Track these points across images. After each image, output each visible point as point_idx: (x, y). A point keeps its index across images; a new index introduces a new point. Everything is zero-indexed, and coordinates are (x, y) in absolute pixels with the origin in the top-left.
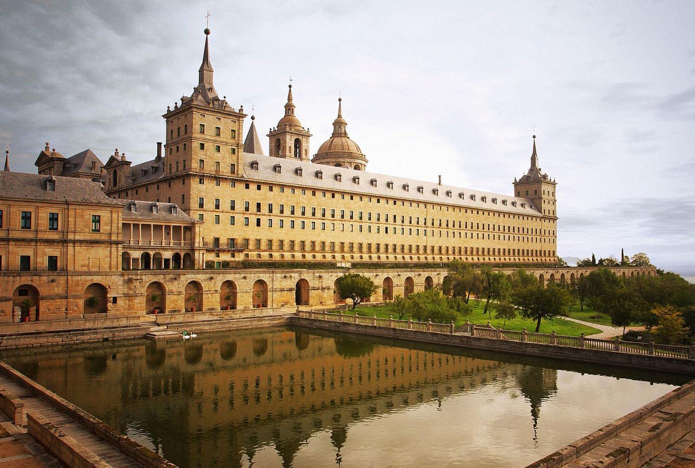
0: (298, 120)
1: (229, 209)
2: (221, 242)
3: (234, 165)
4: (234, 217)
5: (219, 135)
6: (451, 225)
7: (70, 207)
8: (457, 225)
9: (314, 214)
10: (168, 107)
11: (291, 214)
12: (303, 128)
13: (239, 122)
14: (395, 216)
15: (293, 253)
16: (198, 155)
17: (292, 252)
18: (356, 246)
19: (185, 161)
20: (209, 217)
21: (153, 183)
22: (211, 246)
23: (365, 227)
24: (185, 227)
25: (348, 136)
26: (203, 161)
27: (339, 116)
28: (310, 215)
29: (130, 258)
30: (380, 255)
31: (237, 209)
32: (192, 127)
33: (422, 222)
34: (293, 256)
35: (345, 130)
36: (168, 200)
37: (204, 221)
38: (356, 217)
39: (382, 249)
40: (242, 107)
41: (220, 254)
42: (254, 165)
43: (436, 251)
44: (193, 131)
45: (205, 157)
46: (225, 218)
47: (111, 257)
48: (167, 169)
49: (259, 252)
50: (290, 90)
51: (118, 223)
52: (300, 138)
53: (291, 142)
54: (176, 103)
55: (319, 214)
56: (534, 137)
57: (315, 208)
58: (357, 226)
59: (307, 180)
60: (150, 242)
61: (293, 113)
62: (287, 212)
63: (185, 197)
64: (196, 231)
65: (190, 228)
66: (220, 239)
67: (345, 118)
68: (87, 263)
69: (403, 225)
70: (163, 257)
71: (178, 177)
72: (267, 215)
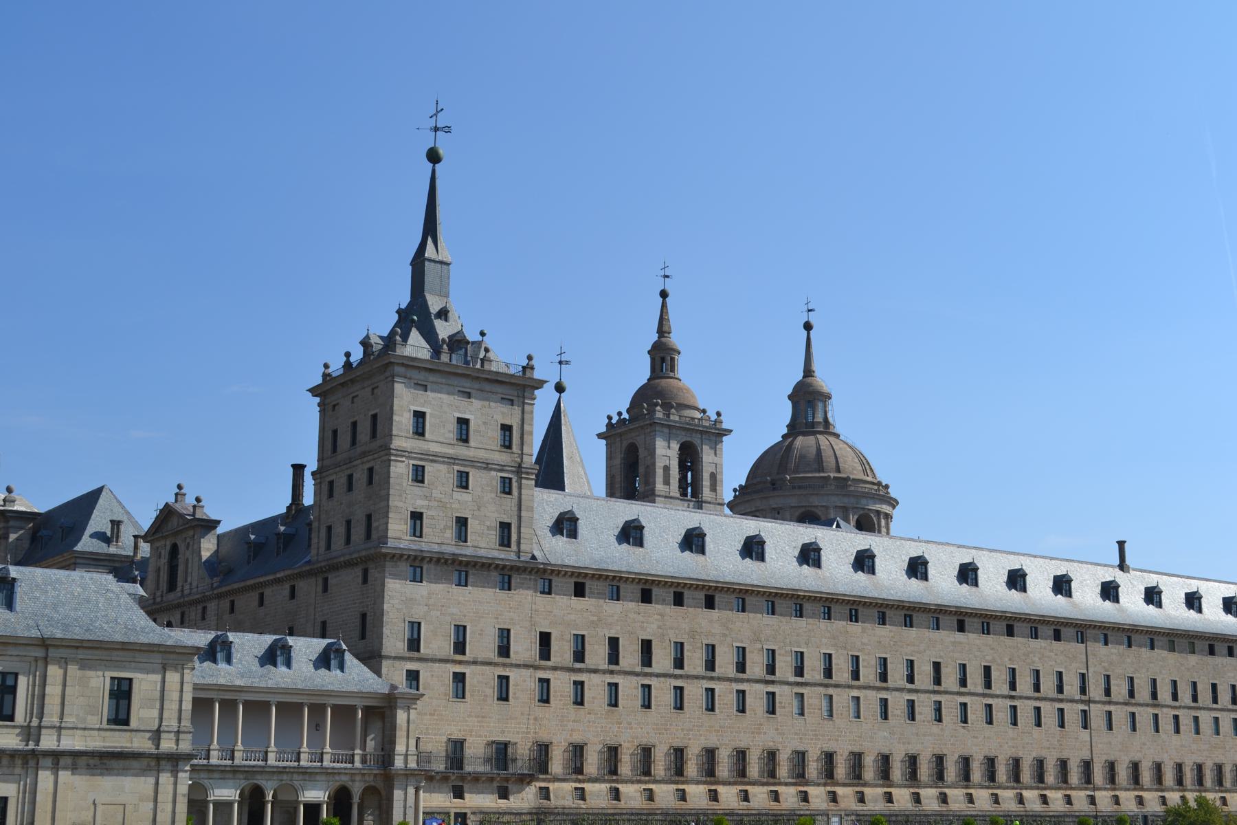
0: (688, 390)
1: (492, 655)
2: (469, 751)
3: (509, 525)
4: (507, 678)
5: (464, 438)
6: (1164, 695)
7: (53, 653)
8: (1185, 696)
9: (741, 667)
10: (326, 366)
11: (675, 667)
12: (704, 411)
13: (524, 403)
14: (987, 670)
15: (681, 787)
16: (403, 497)
17: (677, 783)
18: (869, 761)
19: (369, 517)
20: (436, 679)
21: (278, 581)
22: (439, 766)
23: (898, 703)
24: (368, 710)
25: (836, 431)
26: (421, 514)
27: (808, 372)
28: (731, 671)
29: (205, 803)
30: (946, 790)
31: (516, 653)
32: (391, 419)
33: (1072, 688)
34: (683, 796)
35: (826, 413)
36: (318, 629)
37: (421, 690)
38: (868, 673)
39: (951, 772)
40: (530, 358)
41: (466, 787)
42: (566, 525)
43: (1123, 775)
44: (394, 432)
45: (425, 503)
46: (481, 680)
47: (156, 801)
48: (318, 540)
49: (580, 781)
50: (664, 305)
51: (181, 701)
52: (696, 440)
53: (669, 453)
54: (348, 355)
55: (756, 667)
57: (744, 649)
58: (870, 700)
59: (722, 561)
60: (266, 753)
61: (672, 370)
62: (662, 660)
63: (369, 618)
64: (398, 721)
65: (381, 713)
66: (466, 745)
67: (824, 379)
68: (90, 819)
69: (1012, 697)
70: (301, 799)
71: (350, 564)
72: (604, 672)
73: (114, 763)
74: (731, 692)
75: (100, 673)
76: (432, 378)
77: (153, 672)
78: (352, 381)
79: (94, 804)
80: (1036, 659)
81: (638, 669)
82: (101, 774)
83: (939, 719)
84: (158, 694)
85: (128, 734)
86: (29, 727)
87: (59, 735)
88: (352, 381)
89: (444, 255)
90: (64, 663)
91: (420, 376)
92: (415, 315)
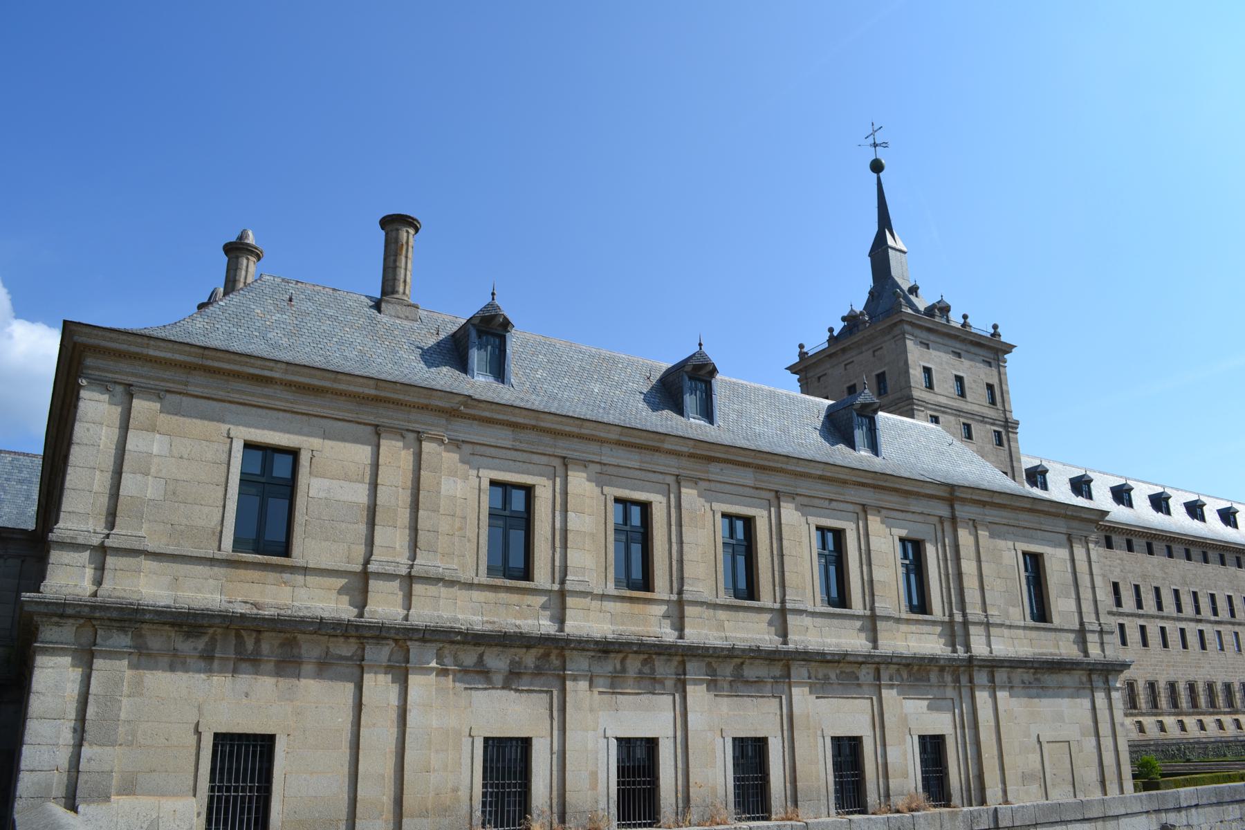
5: (962, 394)
7: (962, 511)
10: (801, 346)
32: (907, 372)
54: (831, 330)
73: (1050, 679)
75: (1010, 544)
76: (932, 337)
77: (1059, 545)
78: (844, 350)
79: (1039, 742)
81: (1115, 609)
82: (1038, 696)
84: (1070, 576)
85: (1052, 635)
86: (951, 622)
87: (988, 636)
88: (844, 350)
89: (900, 245)
90: (974, 525)
91: (924, 335)
92: (885, 289)
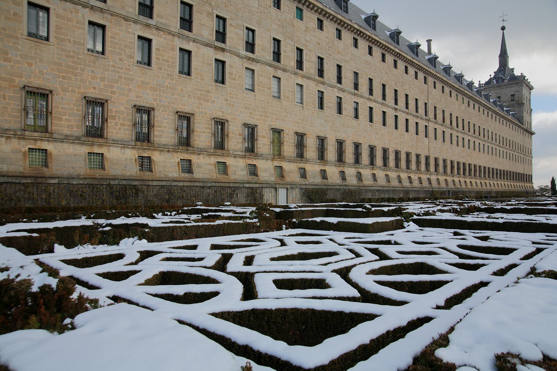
18: (311, 144)
30: (361, 171)
56: (503, 28)
58: (312, 89)
69: (396, 109)
74: (173, 49)
80: (407, 87)
83: (356, 117)
